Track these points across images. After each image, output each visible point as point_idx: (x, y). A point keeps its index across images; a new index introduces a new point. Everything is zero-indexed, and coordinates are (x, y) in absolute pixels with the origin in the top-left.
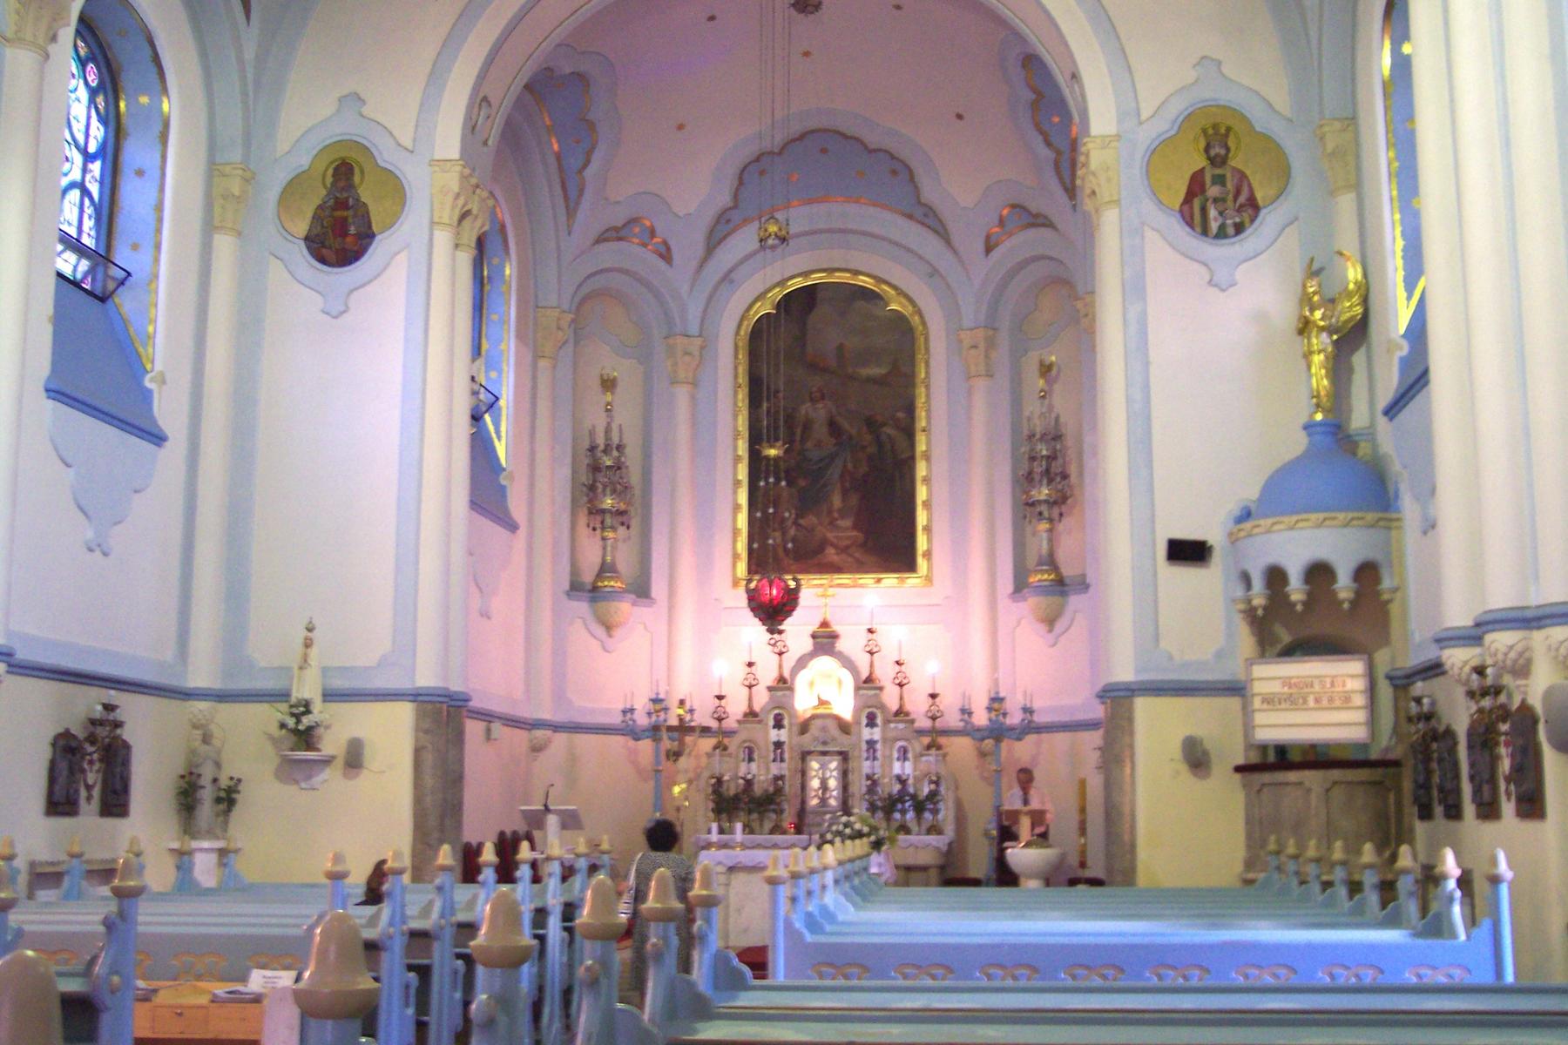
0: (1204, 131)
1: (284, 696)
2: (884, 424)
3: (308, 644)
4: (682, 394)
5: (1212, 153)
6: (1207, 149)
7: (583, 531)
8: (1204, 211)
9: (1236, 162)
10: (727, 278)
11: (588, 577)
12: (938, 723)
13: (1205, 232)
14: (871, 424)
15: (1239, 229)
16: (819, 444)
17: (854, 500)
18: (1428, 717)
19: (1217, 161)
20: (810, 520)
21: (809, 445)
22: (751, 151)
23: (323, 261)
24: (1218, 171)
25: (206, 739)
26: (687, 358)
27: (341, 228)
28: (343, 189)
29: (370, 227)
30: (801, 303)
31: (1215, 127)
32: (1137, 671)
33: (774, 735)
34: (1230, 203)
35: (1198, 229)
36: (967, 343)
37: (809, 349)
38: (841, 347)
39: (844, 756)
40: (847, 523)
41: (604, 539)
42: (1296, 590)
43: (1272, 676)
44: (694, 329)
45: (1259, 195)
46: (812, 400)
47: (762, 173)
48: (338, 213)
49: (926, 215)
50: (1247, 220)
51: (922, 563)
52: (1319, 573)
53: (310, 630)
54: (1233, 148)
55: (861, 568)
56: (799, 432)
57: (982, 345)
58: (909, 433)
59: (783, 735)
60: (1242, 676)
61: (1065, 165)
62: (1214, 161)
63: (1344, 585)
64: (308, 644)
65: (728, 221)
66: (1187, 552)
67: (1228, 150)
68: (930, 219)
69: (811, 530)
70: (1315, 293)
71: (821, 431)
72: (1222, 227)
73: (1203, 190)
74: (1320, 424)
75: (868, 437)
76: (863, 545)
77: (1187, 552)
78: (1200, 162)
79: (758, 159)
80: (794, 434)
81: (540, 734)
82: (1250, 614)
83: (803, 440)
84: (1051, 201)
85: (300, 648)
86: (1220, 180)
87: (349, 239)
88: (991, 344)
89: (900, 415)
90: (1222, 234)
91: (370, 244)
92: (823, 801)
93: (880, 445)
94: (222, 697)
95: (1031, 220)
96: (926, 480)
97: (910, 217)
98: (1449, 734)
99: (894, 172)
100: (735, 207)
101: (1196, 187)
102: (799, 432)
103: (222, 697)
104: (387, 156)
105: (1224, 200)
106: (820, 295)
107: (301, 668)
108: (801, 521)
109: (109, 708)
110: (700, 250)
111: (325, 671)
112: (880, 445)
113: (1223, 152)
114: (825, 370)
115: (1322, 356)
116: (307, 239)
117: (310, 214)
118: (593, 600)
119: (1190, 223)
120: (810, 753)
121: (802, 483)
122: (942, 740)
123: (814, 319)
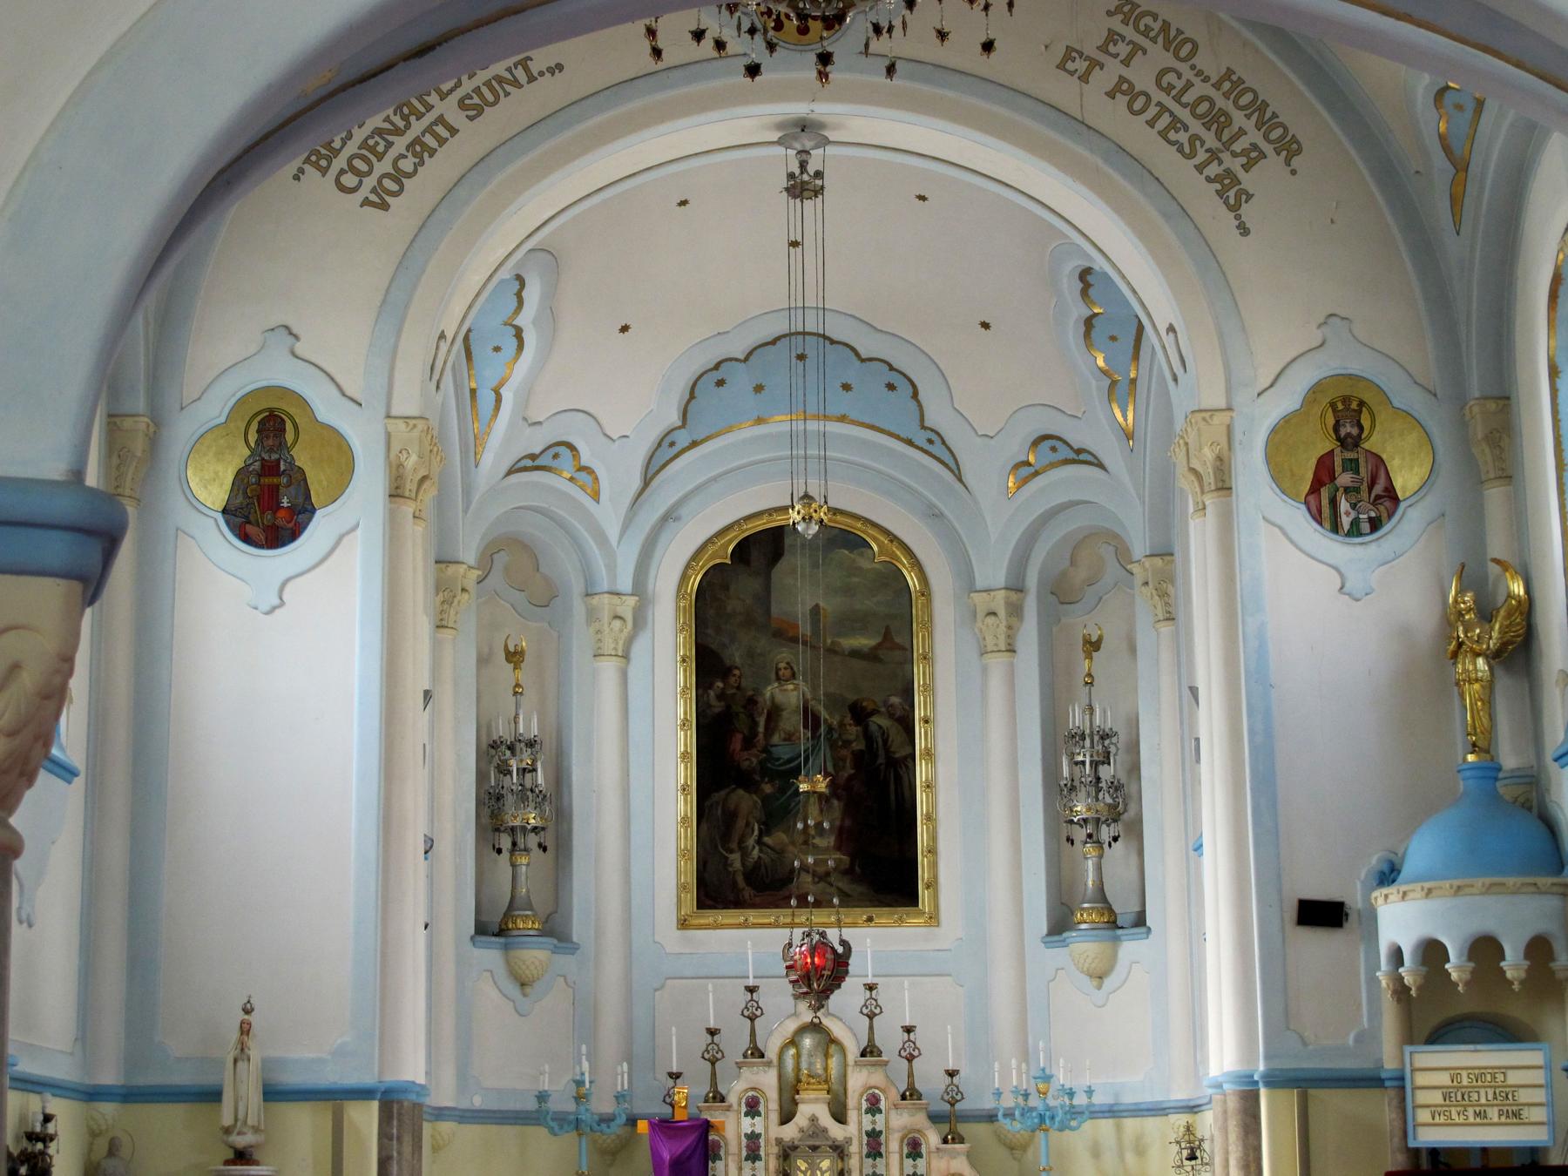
0: (1333, 405)
2: (875, 712)
5: (1343, 432)
6: (1336, 429)
8: (1334, 503)
9: (1372, 443)
11: (495, 919)
12: (958, 1106)
13: (1335, 528)
14: (860, 713)
15: (1375, 525)
16: (790, 738)
19: (1350, 443)
20: (777, 838)
21: (776, 739)
23: (246, 538)
24: (1350, 455)
25: (113, 1151)
26: (617, 624)
27: (269, 498)
28: (271, 450)
29: (308, 496)
30: (760, 549)
31: (1346, 400)
32: (1267, 1057)
33: (747, 1125)
34: (1364, 494)
35: (1327, 525)
37: (774, 610)
38: (816, 610)
40: (827, 842)
41: (514, 865)
42: (1456, 966)
43: (1437, 1068)
44: (625, 583)
45: (1398, 484)
46: (778, 679)
47: (720, 383)
48: (266, 481)
49: (930, 441)
50: (1385, 515)
51: (924, 894)
52: (1485, 949)
53: (247, 1012)
54: (1366, 422)
55: (848, 901)
56: (762, 721)
57: (1002, 612)
58: (906, 725)
59: (758, 1125)
62: (1342, 442)
63: (1513, 964)
65: (672, 444)
66: (1321, 914)
67: (1361, 428)
68: (935, 445)
69: (780, 852)
70: (1469, 610)
72: (1355, 523)
73: (1333, 478)
74: (1473, 767)
75: (853, 731)
76: (848, 872)
77: (1321, 914)
78: (1326, 444)
79: (717, 367)
80: (755, 724)
81: (446, 1127)
82: (1401, 991)
85: (234, 1035)
86: (1352, 466)
87: (281, 514)
89: (895, 700)
90: (1355, 531)
91: (310, 520)
93: (868, 736)
94: (130, 1095)
95: (1072, 455)
96: (928, 786)
97: (910, 443)
99: (891, 387)
100: (684, 425)
101: (1324, 474)
102: (762, 721)
103: (130, 1095)
104: (327, 408)
105: (1357, 490)
106: (788, 541)
107: (235, 1061)
108: (766, 839)
109: (47, 1119)
110: (637, 483)
112: (868, 736)
113: (1355, 431)
114: (795, 640)
115: (1477, 686)
116: (224, 511)
118: (506, 948)
119: (1318, 518)
120: (795, 1148)
121: (768, 789)
122: (963, 1128)
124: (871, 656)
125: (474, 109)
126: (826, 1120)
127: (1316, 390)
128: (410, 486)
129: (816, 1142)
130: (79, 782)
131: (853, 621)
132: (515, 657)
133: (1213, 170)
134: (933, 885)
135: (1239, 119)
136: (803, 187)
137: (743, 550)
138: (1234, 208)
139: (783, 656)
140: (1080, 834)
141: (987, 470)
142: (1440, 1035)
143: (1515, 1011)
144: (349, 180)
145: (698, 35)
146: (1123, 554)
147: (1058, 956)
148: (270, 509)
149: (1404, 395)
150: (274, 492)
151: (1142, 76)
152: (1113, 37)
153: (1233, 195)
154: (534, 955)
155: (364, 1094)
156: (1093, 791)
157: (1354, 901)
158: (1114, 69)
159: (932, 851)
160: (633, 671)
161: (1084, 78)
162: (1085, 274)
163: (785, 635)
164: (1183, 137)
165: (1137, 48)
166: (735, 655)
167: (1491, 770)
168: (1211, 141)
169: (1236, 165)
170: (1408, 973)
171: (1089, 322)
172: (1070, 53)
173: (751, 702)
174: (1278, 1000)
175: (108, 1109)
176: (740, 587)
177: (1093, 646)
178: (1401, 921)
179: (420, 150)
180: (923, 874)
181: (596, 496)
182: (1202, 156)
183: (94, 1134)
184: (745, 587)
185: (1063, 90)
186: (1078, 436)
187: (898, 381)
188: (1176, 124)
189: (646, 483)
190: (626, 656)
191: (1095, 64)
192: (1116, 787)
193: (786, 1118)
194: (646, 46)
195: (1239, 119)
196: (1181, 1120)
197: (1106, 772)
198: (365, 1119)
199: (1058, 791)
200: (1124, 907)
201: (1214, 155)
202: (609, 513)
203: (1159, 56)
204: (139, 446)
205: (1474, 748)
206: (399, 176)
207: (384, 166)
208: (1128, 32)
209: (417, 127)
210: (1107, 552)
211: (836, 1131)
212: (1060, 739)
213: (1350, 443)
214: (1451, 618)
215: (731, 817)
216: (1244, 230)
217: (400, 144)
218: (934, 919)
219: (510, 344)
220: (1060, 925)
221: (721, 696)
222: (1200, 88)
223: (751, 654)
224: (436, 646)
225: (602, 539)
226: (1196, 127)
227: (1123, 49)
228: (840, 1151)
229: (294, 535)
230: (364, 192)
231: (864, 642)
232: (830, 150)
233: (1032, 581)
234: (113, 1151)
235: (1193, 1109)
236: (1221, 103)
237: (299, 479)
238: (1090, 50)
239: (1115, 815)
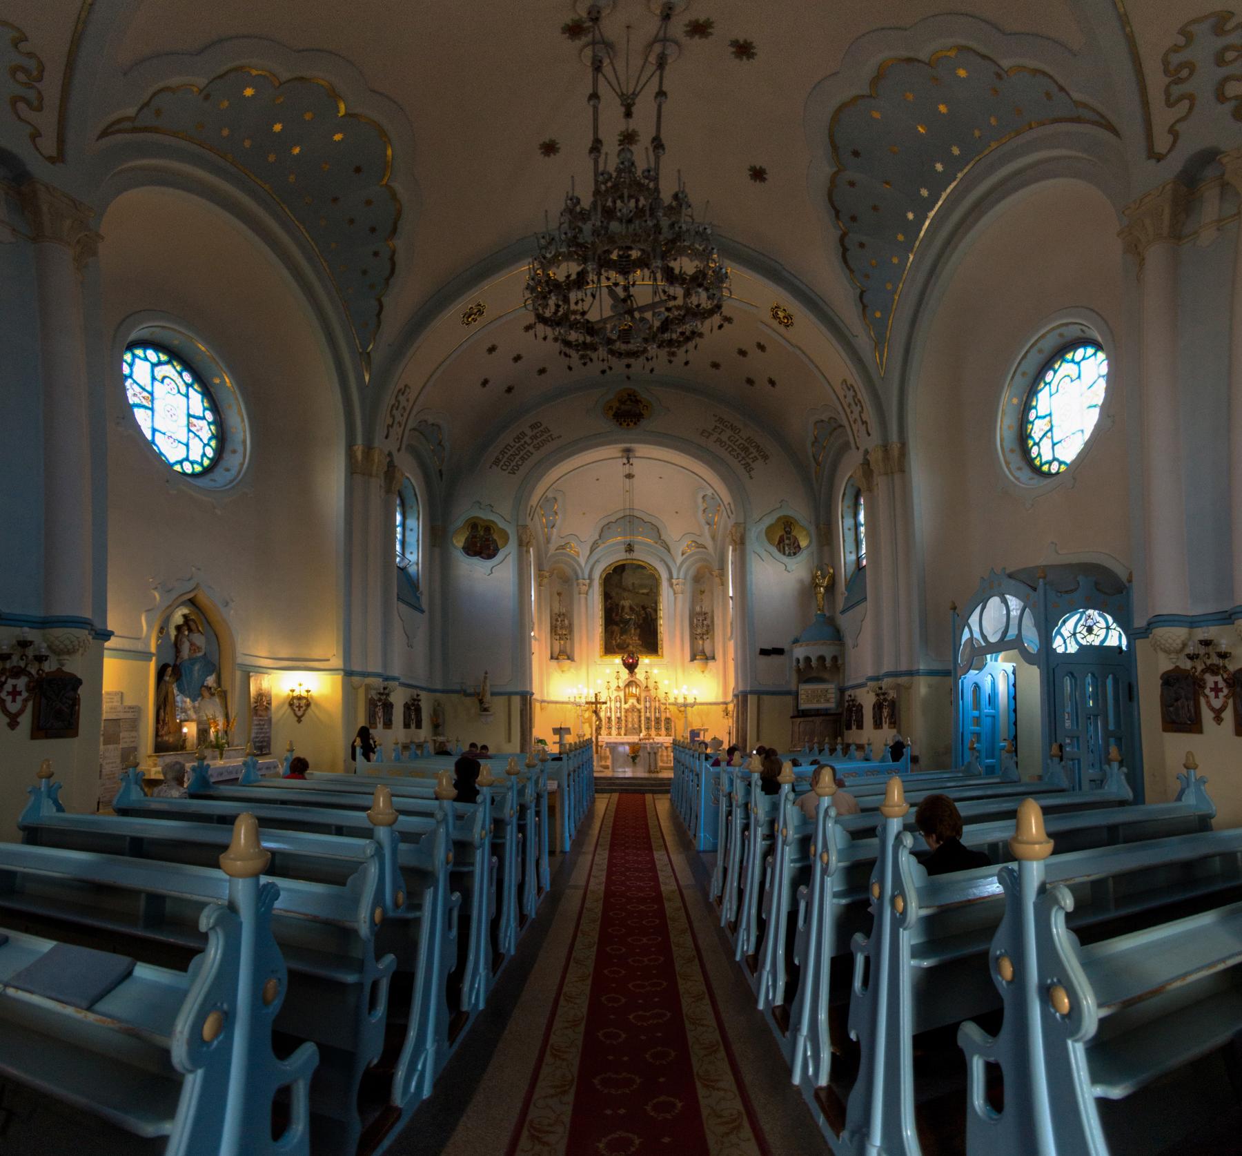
3: (485, 678)
4: (583, 596)
10: (598, 561)
11: (555, 655)
14: (644, 608)
30: (619, 569)
42: (814, 663)
44: (586, 576)
52: (822, 659)
58: (656, 611)
60: (794, 688)
63: (828, 663)
71: (627, 610)
82: (799, 670)
123: (624, 575)
124: (647, 594)
129: (633, 709)
131: (642, 586)
137: (615, 569)
139: (625, 594)
143: (826, 676)
151: (724, 438)
153: (748, 468)
155: (516, 693)
160: (590, 598)
166: (614, 594)
170: (802, 665)
172: (704, 431)
176: (615, 580)
178: (800, 652)
188: (733, 450)
189: (591, 552)
191: (710, 434)
198: (516, 700)
200: (708, 653)
203: (729, 432)
211: (638, 706)
212: (693, 615)
215: (612, 633)
220: (693, 659)
228: (639, 711)
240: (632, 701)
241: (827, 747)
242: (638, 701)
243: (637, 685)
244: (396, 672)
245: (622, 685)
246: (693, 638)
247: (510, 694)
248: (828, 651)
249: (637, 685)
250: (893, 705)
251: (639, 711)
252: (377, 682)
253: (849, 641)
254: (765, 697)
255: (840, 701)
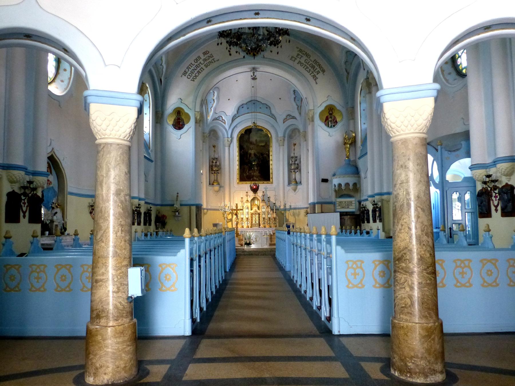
1: (173, 205)
3: (177, 196)
7: (211, 174)
11: (211, 183)
13: (328, 126)
15: (334, 126)
17: (259, 168)
18: (364, 207)
19: (331, 114)
22: (241, 104)
23: (176, 129)
30: (248, 131)
36: (279, 139)
38: (256, 140)
39: (259, 214)
42: (343, 187)
44: (229, 136)
51: (271, 180)
52: (347, 184)
60: (334, 201)
61: (299, 108)
62: (330, 114)
63: (351, 187)
64: (177, 196)
66: (325, 181)
71: (253, 156)
75: (261, 157)
77: (325, 181)
78: (327, 114)
82: (335, 191)
83: (250, 156)
84: (296, 114)
86: (331, 117)
88: (284, 140)
90: (331, 127)
92: (256, 222)
98: (368, 211)
101: (327, 119)
104: (186, 110)
110: (231, 122)
111: (181, 201)
117: (173, 120)
119: (326, 125)
124: (264, 146)
125: (207, 67)
126: (257, 210)
127: (326, 107)
128: (198, 121)
129: (256, 213)
130: (154, 163)
131: (261, 141)
132: (214, 146)
133: (312, 75)
134: (272, 178)
135: (316, 67)
136: (254, 79)
138: (315, 80)
139: (251, 146)
140: (293, 171)
141: (280, 120)
142: (342, 196)
143: (352, 193)
144: (189, 77)
145: (237, 52)
146: (299, 131)
147: (289, 188)
148: (179, 125)
149: (338, 107)
150: (179, 122)
151: (303, 61)
152: (298, 55)
153: (315, 78)
154: (217, 188)
156: (294, 166)
157: (329, 179)
158: (298, 59)
159: (272, 173)
161: (294, 61)
162: (294, 91)
163: (251, 143)
164: (308, 70)
165: (302, 56)
167: (349, 160)
168: (312, 70)
169: (316, 74)
171: (295, 98)
172: (292, 57)
173: (247, 153)
174: (318, 192)
175: (159, 207)
177: (295, 145)
178: (336, 181)
179: (199, 72)
180: (271, 177)
181: (225, 123)
182: (311, 72)
183: (157, 210)
184: (246, 137)
185: (291, 63)
186: (293, 115)
187: (268, 107)
188: (307, 68)
190: (230, 146)
191: (296, 59)
192: (298, 164)
193: (251, 210)
194: (228, 53)
195: (316, 67)
196: (306, 209)
197: (296, 162)
198: (194, 208)
199: (289, 165)
200: (298, 180)
201: (312, 72)
202: (227, 126)
203: (305, 58)
204: (160, 115)
205: (347, 157)
206: (196, 76)
207: (194, 75)
208: (301, 54)
209: (198, 69)
210: (297, 131)
211: (259, 211)
212: (290, 158)
213: (331, 114)
214: (345, 139)
216: (317, 83)
217: (196, 71)
218: (272, 183)
219: (213, 102)
220: (289, 183)
221: (243, 152)
222: (311, 63)
223: (247, 146)
224: (203, 145)
225: (226, 129)
226: (310, 68)
227: (300, 57)
229: (182, 128)
230: (191, 78)
231: (263, 144)
232: (257, 72)
233: (286, 136)
234: (159, 213)
235: (307, 208)
236: (314, 64)
237: (183, 120)
238: (295, 57)
239: (297, 168)
240: (255, 208)
241: (353, 231)
242: (258, 208)
243: (258, 200)
244: (142, 196)
245: (250, 200)
246: (290, 171)
247: (190, 205)
248: (351, 180)
249: (258, 200)
250: (380, 209)
251: (259, 214)
252: (136, 202)
253: (362, 175)
254: (325, 205)
255: (360, 208)
